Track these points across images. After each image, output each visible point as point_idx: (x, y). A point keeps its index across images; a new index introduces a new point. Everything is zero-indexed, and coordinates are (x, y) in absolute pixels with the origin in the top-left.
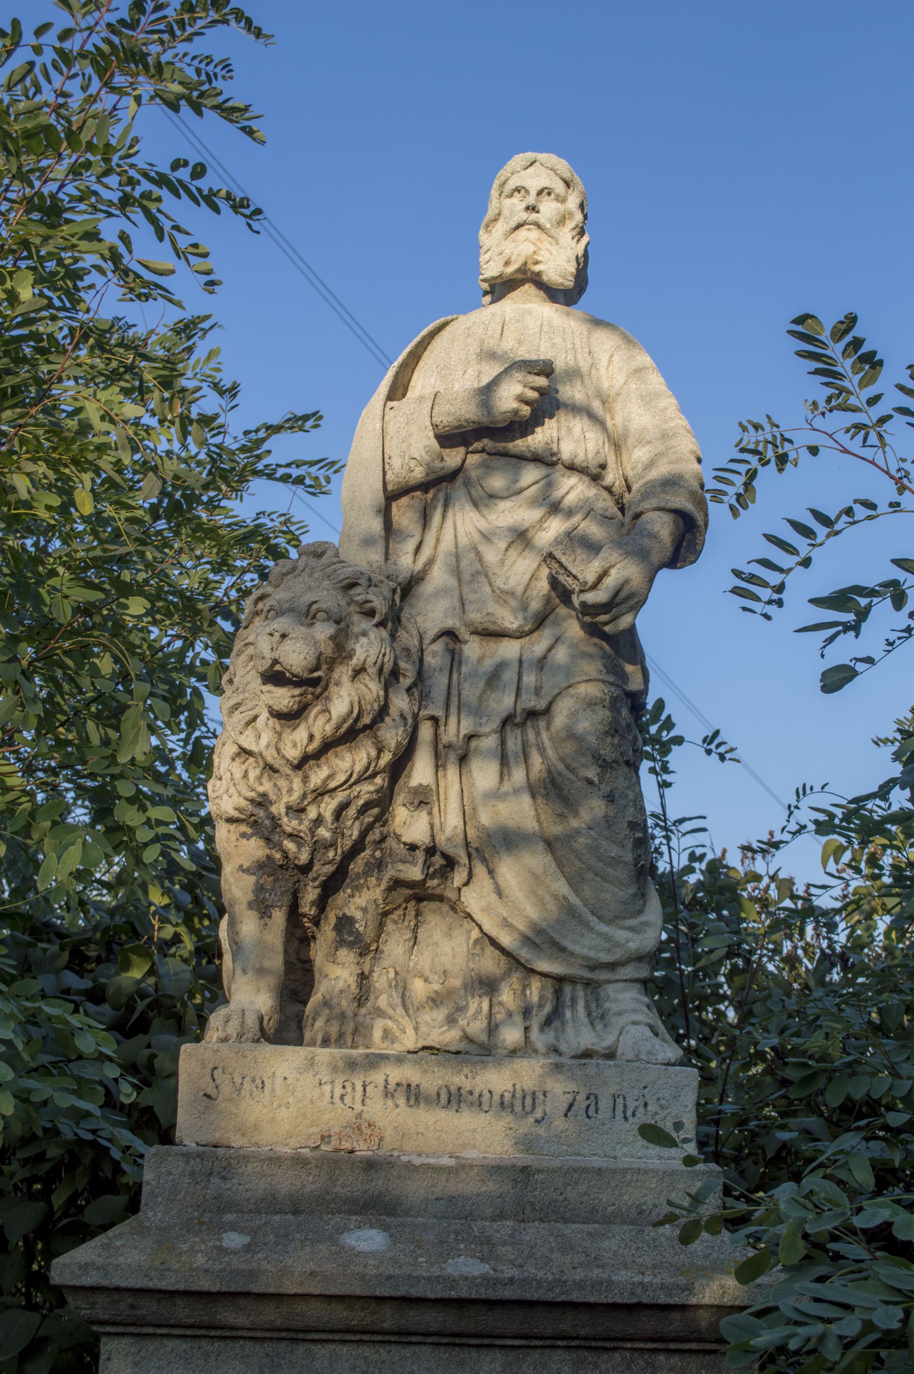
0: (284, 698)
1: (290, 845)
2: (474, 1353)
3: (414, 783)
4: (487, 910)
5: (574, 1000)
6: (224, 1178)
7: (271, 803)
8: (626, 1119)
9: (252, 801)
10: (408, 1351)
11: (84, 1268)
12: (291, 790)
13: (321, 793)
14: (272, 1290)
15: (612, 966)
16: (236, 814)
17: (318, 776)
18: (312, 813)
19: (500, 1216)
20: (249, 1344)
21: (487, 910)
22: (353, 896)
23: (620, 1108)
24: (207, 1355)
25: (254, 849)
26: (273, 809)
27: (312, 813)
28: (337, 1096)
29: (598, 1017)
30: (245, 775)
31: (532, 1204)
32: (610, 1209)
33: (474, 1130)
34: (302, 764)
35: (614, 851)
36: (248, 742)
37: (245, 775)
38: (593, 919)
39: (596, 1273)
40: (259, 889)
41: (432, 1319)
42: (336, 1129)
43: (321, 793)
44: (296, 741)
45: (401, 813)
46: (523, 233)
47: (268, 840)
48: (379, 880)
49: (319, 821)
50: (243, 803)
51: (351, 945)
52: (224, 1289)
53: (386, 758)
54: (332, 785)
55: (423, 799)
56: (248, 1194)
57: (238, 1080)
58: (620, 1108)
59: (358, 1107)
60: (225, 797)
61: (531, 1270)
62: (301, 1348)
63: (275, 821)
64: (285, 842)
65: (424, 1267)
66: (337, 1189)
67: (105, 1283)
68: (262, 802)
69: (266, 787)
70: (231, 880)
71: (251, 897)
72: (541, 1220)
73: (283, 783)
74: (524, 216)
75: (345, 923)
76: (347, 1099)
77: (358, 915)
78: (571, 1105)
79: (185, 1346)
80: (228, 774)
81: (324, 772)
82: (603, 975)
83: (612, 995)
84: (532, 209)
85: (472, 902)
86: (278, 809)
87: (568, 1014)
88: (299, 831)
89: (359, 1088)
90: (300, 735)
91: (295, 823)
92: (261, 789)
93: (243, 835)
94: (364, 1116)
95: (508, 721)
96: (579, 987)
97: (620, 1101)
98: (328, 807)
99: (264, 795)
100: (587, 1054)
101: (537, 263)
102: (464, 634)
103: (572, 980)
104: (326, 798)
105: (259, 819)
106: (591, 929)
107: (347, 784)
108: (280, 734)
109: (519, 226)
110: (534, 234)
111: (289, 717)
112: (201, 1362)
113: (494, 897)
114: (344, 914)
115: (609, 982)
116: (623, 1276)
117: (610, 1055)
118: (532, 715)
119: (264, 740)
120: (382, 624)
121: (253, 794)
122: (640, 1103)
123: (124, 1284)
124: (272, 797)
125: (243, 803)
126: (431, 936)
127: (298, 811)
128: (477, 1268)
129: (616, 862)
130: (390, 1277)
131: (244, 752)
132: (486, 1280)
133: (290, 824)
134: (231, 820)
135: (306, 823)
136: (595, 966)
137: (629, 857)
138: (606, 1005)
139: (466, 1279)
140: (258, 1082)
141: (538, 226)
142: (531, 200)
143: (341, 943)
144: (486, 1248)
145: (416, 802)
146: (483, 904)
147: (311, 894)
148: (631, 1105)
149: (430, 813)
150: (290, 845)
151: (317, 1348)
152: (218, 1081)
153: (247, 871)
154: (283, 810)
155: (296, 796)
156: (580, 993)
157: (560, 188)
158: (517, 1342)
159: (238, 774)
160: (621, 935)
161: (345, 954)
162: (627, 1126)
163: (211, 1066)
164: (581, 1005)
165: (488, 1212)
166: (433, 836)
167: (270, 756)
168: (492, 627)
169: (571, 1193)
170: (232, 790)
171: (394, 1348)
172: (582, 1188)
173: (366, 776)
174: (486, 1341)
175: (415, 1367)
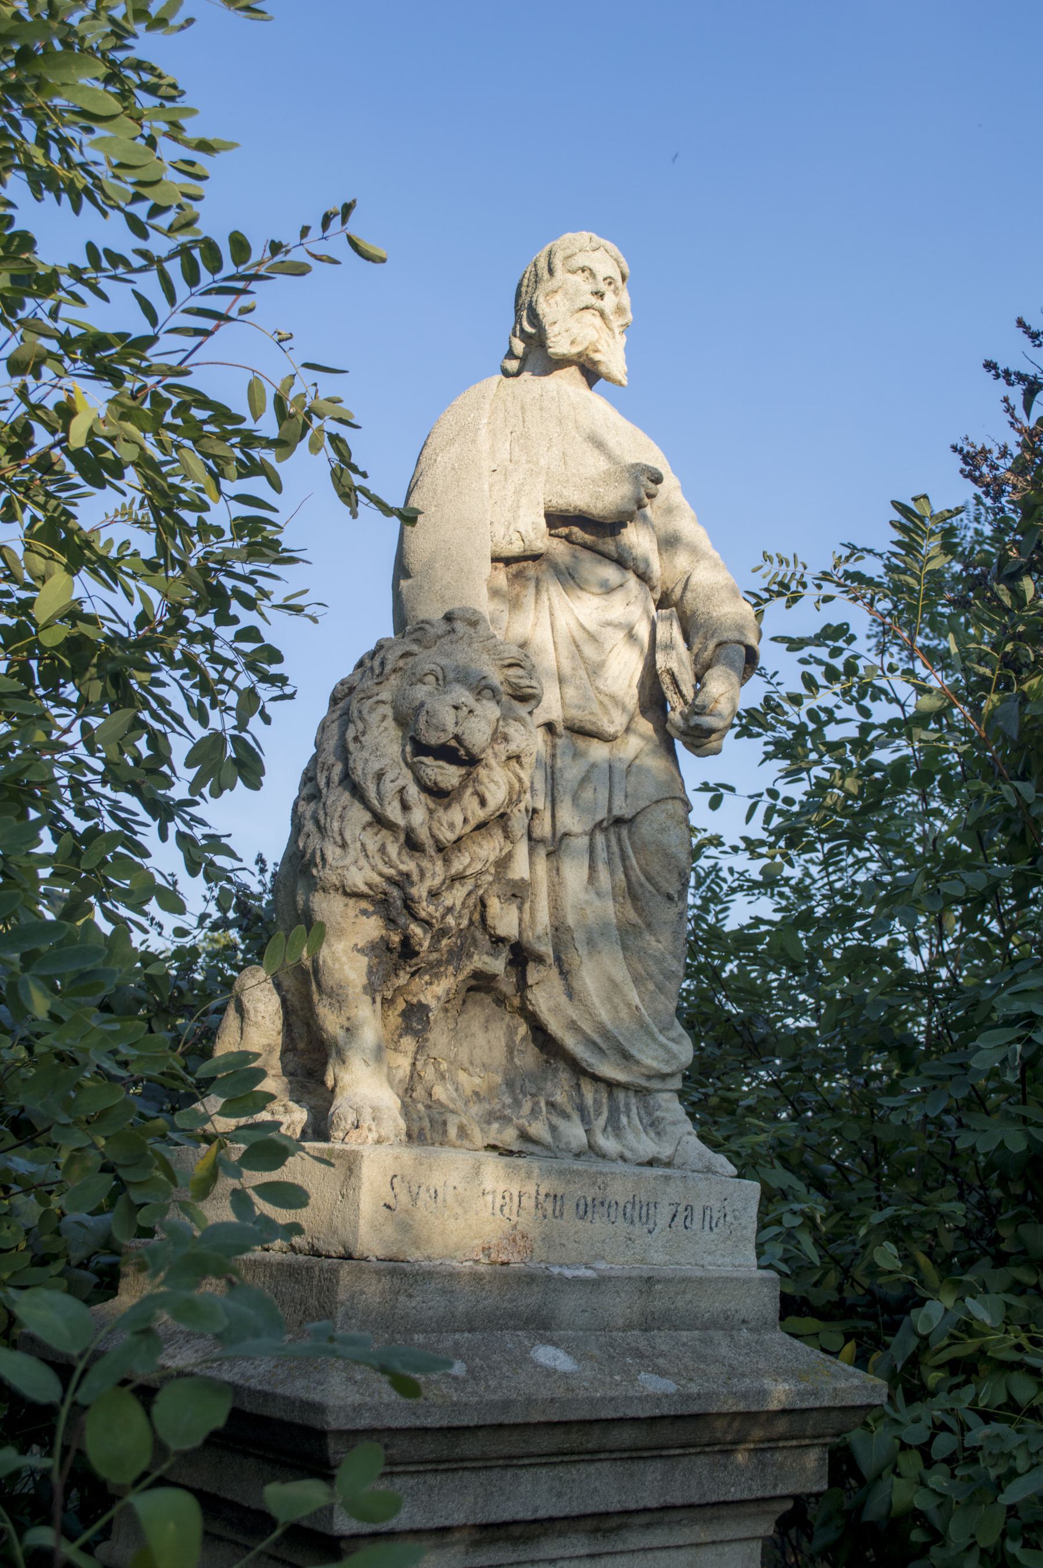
1: (416, 929)
2: (641, 1464)
3: (517, 877)
4: (555, 1010)
5: (627, 1105)
6: (410, 1296)
7: (412, 884)
8: (711, 1229)
9: (389, 880)
10: (592, 1469)
14: (520, 1420)
16: (364, 889)
19: (629, 1327)
20: (467, 1473)
21: (555, 1010)
22: (431, 984)
23: (707, 1218)
24: (431, 1488)
25: (372, 928)
26: (414, 891)
28: (498, 1206)
29: (655, 1126)
30: (382, 850)
31: (653, 1313)
32: (707, 1315)
33: (604, 1241)
37: (382, 850)
41: (625, 1436)
42: (494, 1241)
45: (494, 905)
46: (588, 316)
47: (391, 922)
48: (458, 969)
49: (449, 910)
50: (377, 879)
51: (417, 1034)
52: (481, 1423)
54: (468, 873)
56: (431, 1313)
57: (415, 1189)
58: (707, 1218)
59: (514, 1218)
60: (353, 869)
62: (509, 1473)
63: (409, 904)
64: (412, 926)
66: (505, 1305)
67: (377, 1424)
69: (409, 865)
70: (344, 959)
71: (364, 980)
72: (659, 1329)
73: (425, 864)
76: (506, 1209)
77: (433, 1003)
78: (674, 1216)
79: (412, 1482)
80: (358, 844)
81: (466, 859)
82: (655, 1084)
83: (663, 1104)
85: (541, 1000)
86: (419, 891)
87: (624, 1120)
88: (432, 917)
89: (516, 1199)
91: (431, 909)
92: (403, 868)
93: (364, 912)
94: (519, 1227)
95: (599, 825)
96: (631, 1094)
97: (708, 1212)
99: (408, 875)
101: (596, 351)
102: (560, 729)
103: (625, 1087)
104: (457, 885)
106: (655, 1040)
108: (431, 812)
109: (587, 308)
110: (598, 321)
112: (425, 1498)
113: (563, 999)
114: (419, 1002)
115: (659, 1091)
118: (619, 821)
121: (392, 872)
122: (722, 1214)
123: (394, 1424)
124: (415, 877)
125: (377, 879)
126: (469, 1026)
127: (434, 895)
128: (666, 1386)
130: (612, 1399)
133: (425, 909)
135: (441, 909)
138: (658, 1113)
139: (667, 1396)
140: (432, 1191)
141: (602, 314)
145: (509, 894)
146: (552, 1003)
148: (716, 1215)
149: (520, 909)
150: (416, 929)
151: (521, 1472)
152: (397, 1190)
153: (361, 951)
154: (425, 894)
155: (437, 881)
156: (633, 1100)
158: (677, 1452)
159: (372, 847)
162: (713, 1236)
163: (392, 1173)
164: (634, 1110)
165: (621, 1322)
166: (520, 933)
168: (589, 727)
169: (680, 1303)
170: (362, 862)
171: (582, 1466)
172: (688, 1297)
174: (655, 1453)
175: (597, 1484)
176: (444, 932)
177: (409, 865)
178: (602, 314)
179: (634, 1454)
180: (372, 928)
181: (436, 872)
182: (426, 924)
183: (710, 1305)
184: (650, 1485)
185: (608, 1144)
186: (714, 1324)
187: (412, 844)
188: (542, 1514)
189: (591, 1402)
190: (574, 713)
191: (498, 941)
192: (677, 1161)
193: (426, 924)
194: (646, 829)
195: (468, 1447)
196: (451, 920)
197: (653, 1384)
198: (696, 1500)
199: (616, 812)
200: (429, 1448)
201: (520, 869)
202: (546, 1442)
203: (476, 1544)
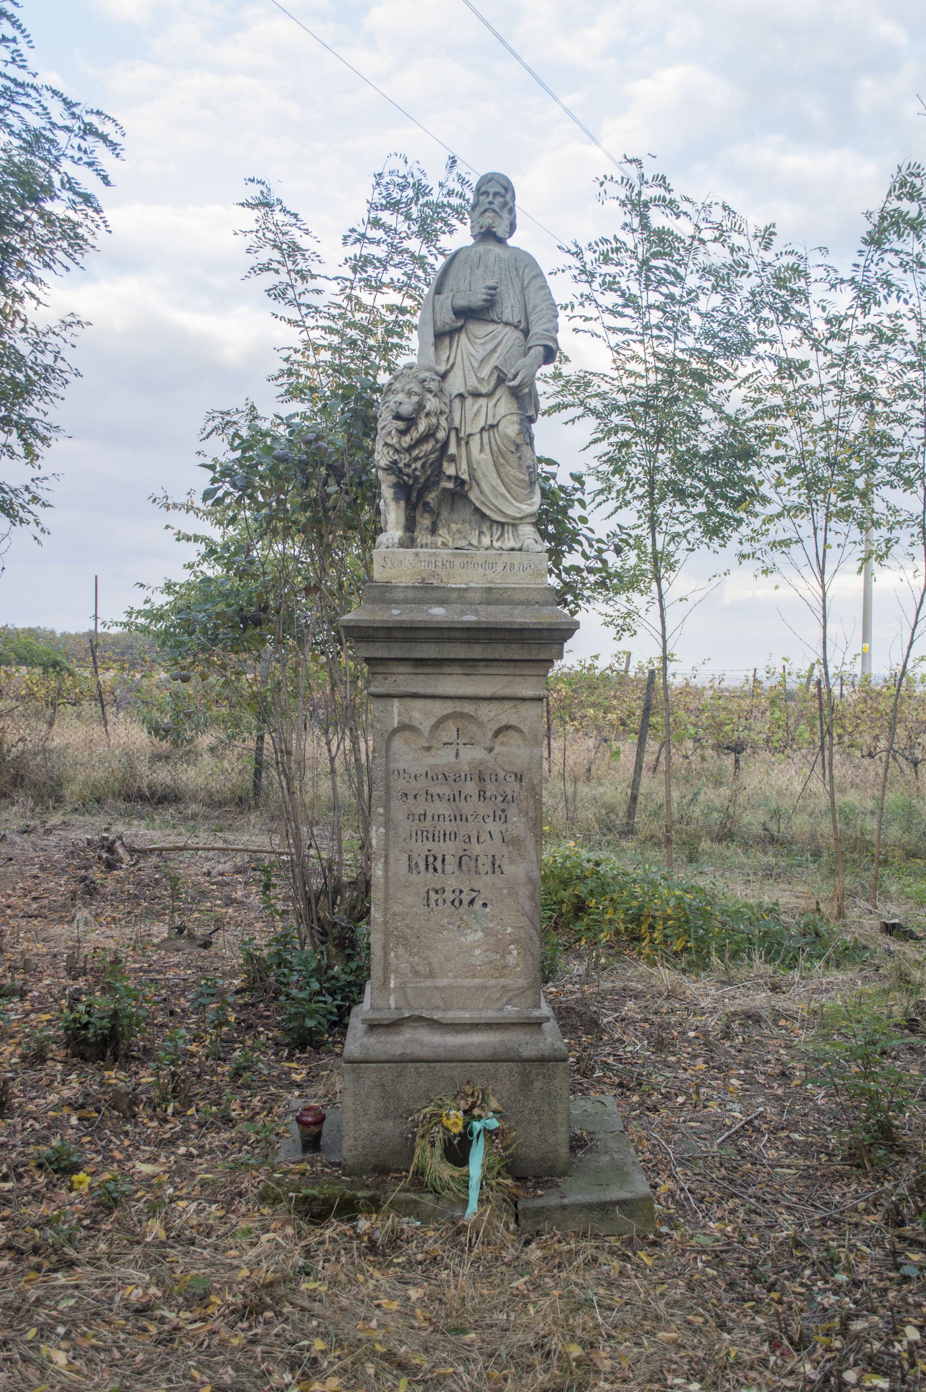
0: (401, 425)
4: (477, 498)
11: (350, 621)
12: (406, 458)
13: (416, 459)
15: (521, 519)
17: (415, 453)
18: (413, 466)
25: (392, 479)
27: (413, 466)
29: (516, 536)
34: (409, 449)
35: (522, 476)
36: (389, 441)
38: (514, 502)
39: (511, 619)
40: (395, 493)
43: (416, 459)
44: (407, 440)
45: (445, 464)
46: (487, 214)
49: (416, 469)
53: (439, 445)
55: (453, 459)
61: (491, 619)
63: (400, 470)
65: (456, 618)
68: (395, 462)
69: (396, 457)
74: (487, 206)
75: (426, 504)
84: (491, 203)
86: (401, 465)
90: (408, 439)
95: (483, 429)
98: (419, 464)
100: (512, 549)
102: (466, 395)
103: (508, 524)
105: (393, 469)
107: (426, 456)
109: (486, 210)
110: (492, 215)
111: (403, 433)
116: (519, 620)
117: (520, 550)
119: (395, 440)
120: (435, 395)
127: (408, 465)
128: (473, 618)
129: (523, 481)
131: (386, 444)
132: (476, 622)
134: (384, 469)
136: (515, 518)
137: (527, 478)
141: (494, 211)
142: (490, 198)
143: (425, 511)
144: (476, 613)
147: (414, 494)
157: (502, 191)
160: (523, 507)
161: (426, 515)
167: (397, 446)
173: (432, 452)
176: (416, 478)
177: (396, 457)
178: (494, 211)
179: (468, 641)
180: (392, 479)
181: (406, 458)
182: (408, 475)
183: (517, 596)
184: (477, 652)
185: (496, 544)
186: (521, 603)
187: (396, 451)
188: (432, 657)
189: (437, 622)
190: (470, 388)
191: (449, 477)
192: (525, 547)
193: (408, 475)
194: (501, 427)
195: (395, 634)
196: (418, 473)
197: (466, 618)
198: (498, 657)
199: (489, 422)
200: (382, 634)
201: (452, 449)
202: (430, 634)
203: (416, 666)
